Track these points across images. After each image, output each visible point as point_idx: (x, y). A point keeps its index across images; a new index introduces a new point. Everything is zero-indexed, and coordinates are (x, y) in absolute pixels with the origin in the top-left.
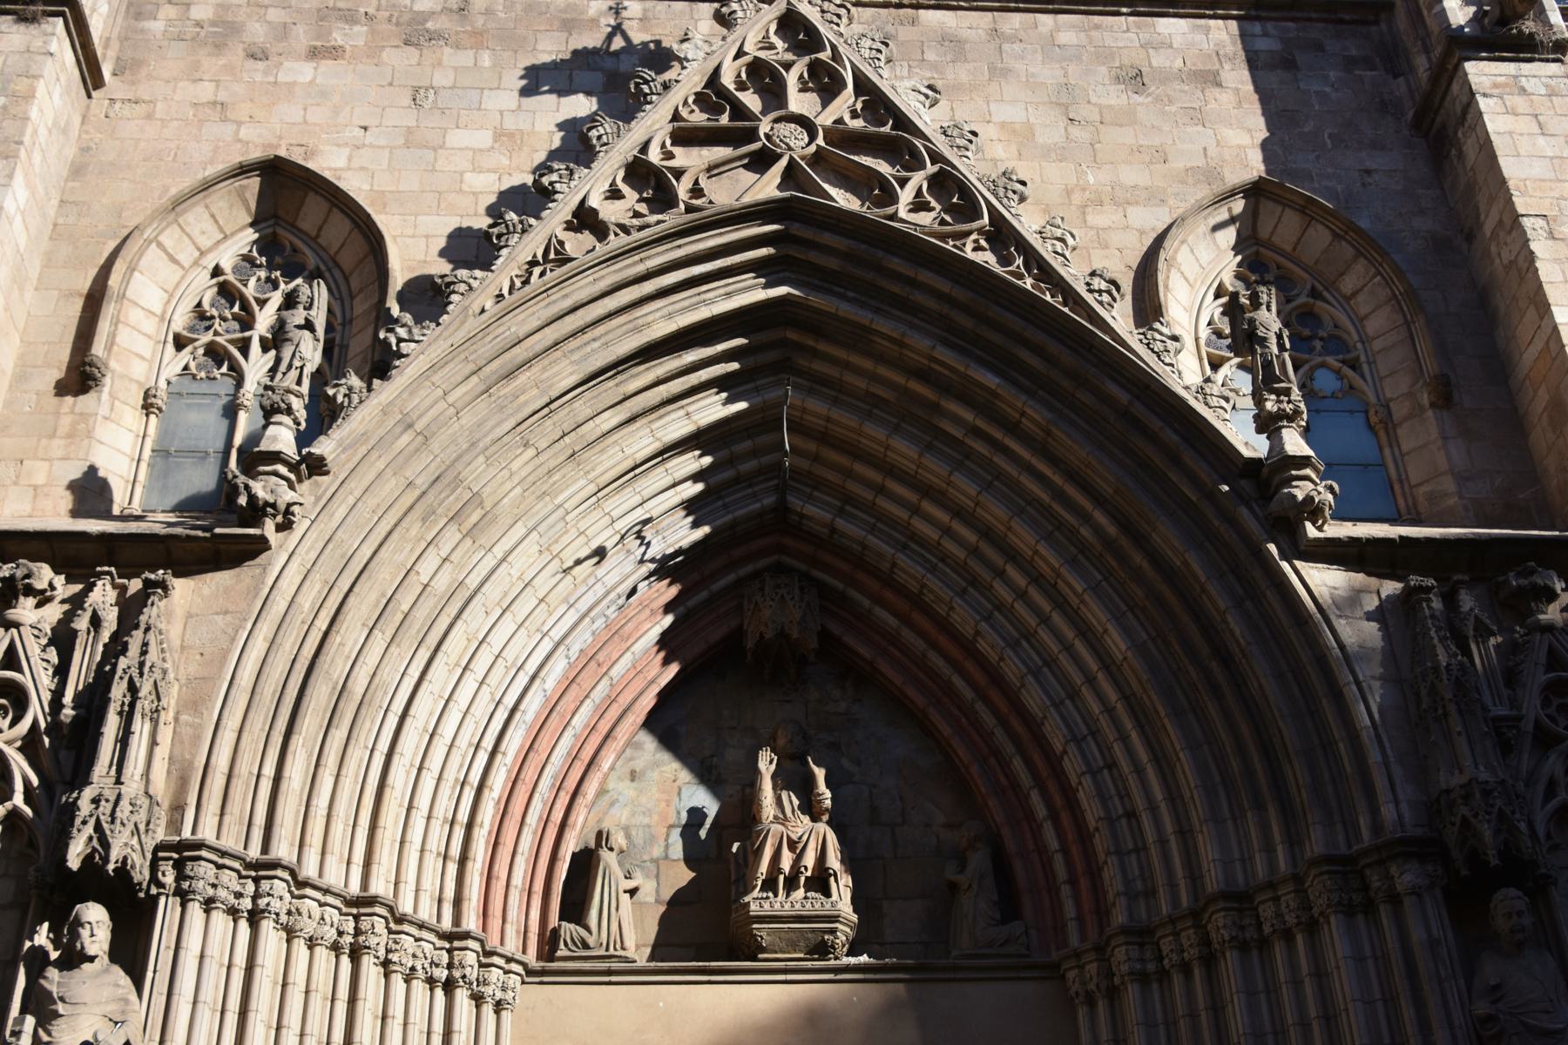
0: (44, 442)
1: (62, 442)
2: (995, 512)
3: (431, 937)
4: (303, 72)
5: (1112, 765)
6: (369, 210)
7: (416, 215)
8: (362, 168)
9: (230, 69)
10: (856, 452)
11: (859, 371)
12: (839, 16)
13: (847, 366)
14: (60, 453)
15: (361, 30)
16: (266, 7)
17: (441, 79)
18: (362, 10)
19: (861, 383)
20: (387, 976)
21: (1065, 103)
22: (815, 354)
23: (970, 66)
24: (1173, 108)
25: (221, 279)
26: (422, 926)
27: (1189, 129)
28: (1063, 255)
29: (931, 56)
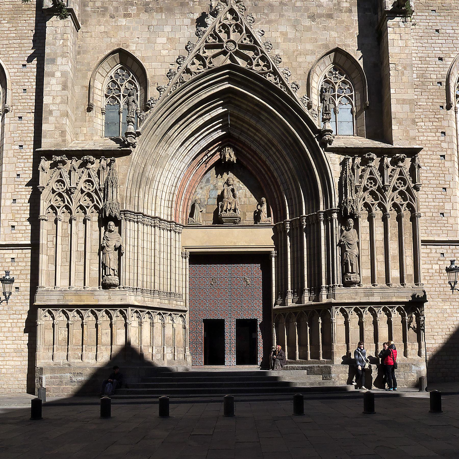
0: (84, 123)
1: (88, 123)
2: (270, 136)
3: (167, 222)
4: (123, 22)
5: (289, 189)
6: (141, 62)
7: (152, 63)
8: (139, 50)
9: (107, 21)
10: (244, 121)
11: (244, 104)
12: (243, 9)
13: (242, 102)
14: (88, 126)
15: (134, 8)
16: (113, 1)
17: (154, 23)
18: (134, 1)
19: (245, 106)
20: (160, 230)
21: (295, 25)
22: (235, 99)
23: (275, 14)
24: (321, 26)
25: (112, 79)
26: (165, 221)
27: (324, 32)
28: (287, 78)
29: (266, 11)
